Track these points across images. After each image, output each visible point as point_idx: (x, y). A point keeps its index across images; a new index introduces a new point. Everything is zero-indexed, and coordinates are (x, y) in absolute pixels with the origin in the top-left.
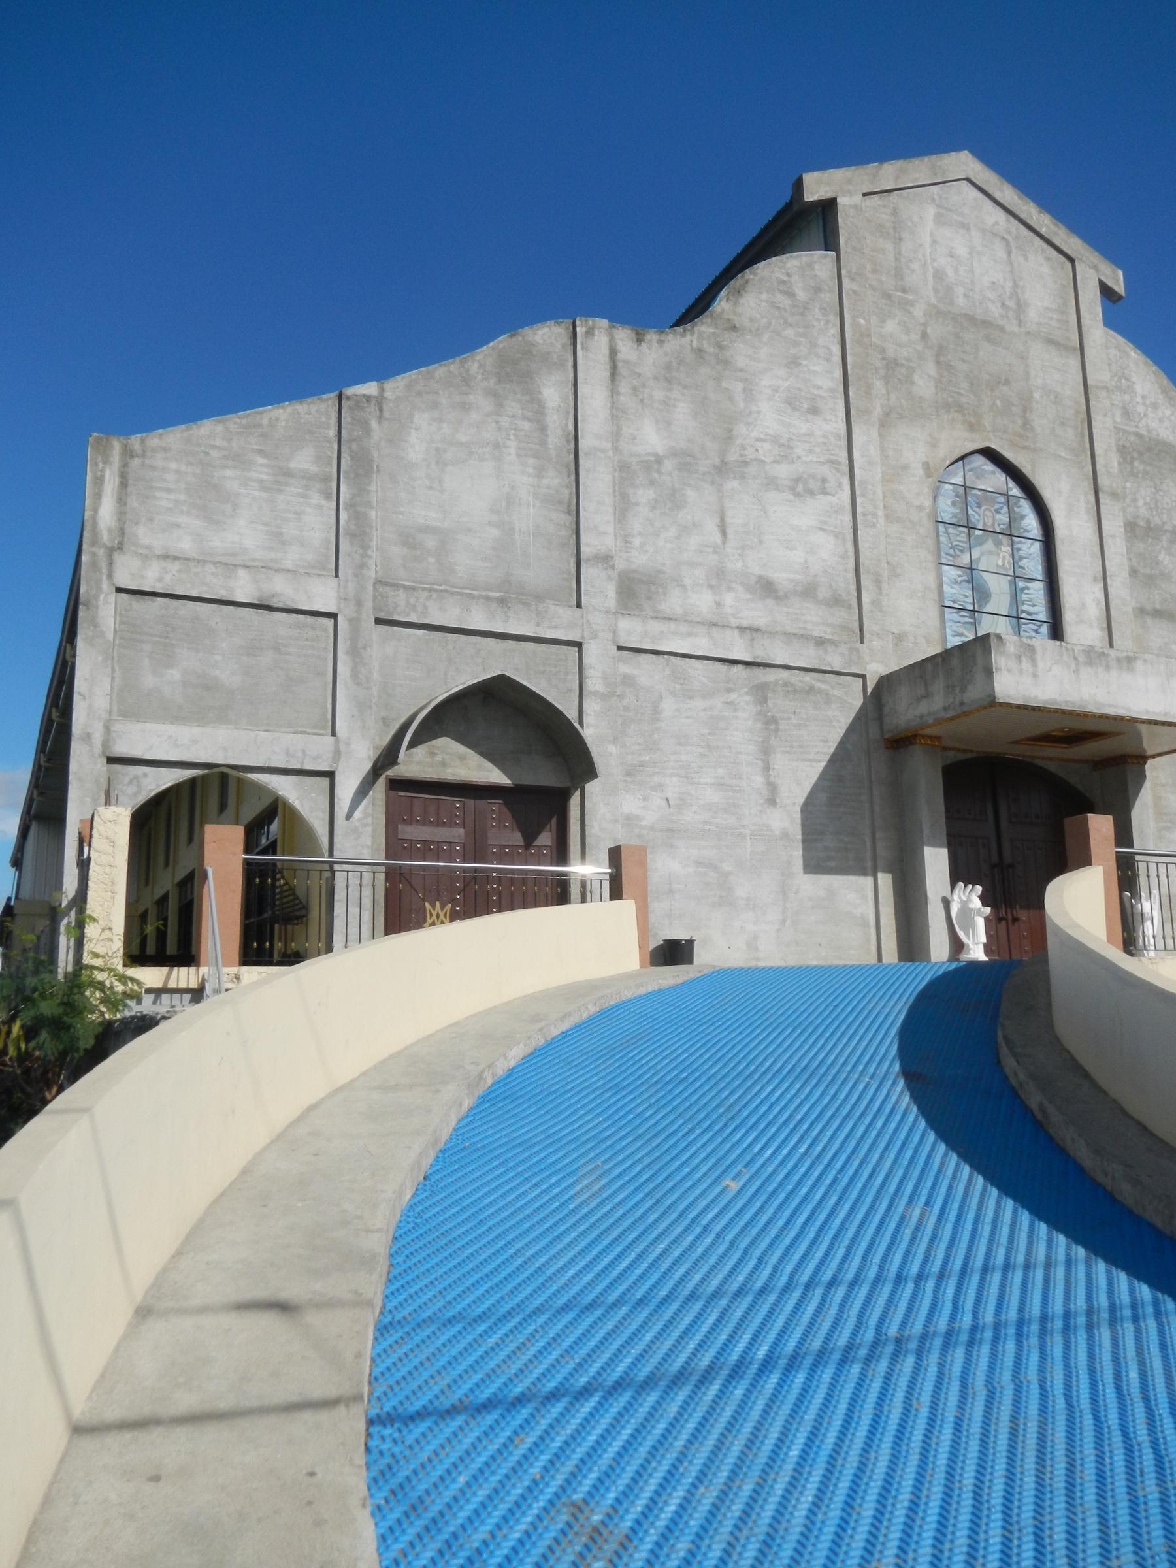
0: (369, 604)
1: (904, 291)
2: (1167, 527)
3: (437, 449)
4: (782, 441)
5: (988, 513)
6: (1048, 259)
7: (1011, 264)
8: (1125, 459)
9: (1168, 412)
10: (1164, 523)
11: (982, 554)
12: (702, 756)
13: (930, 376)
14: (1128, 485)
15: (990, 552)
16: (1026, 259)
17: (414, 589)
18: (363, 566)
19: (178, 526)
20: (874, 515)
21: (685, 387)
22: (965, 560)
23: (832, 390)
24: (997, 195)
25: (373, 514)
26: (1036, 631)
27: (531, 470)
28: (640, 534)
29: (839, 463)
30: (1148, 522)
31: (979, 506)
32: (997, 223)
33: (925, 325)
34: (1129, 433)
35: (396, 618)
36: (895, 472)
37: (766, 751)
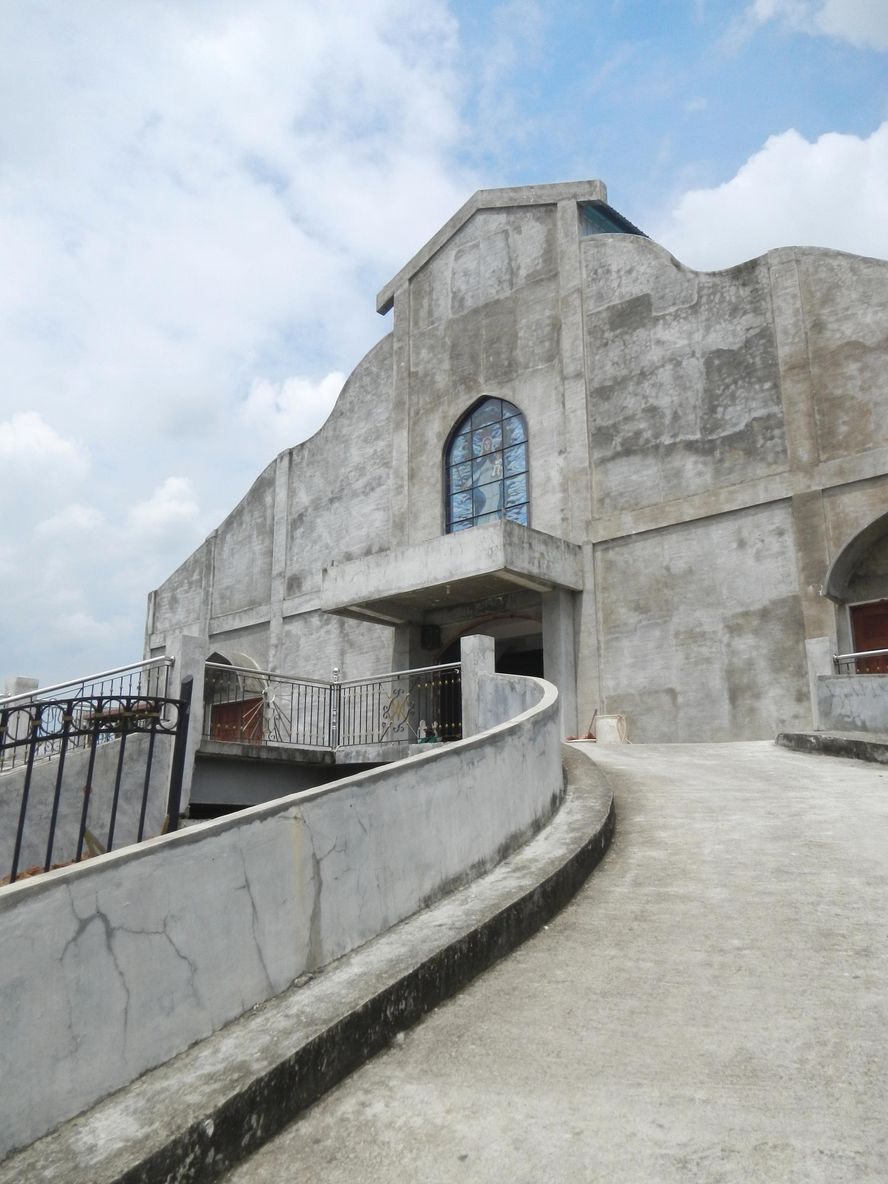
0: (207, 630)
1: (433, 323)
2: (633, 374)
3: (232, 549)
4: (361, 466)
5: (487, 442)
6: (538, 219)
7: (508, 246)
8: (596, 338)
9: (642, 269)
10: (631, 372)
11: (481, 474)
12: (315, 664)
13: (445, 371)
14: (597, 357)
15: (487, 470)
16: (520, 232)
17: (219, 617)
18: (207, 614)
19: (165, 618)
20: (402, 486)
21: (319, 462)
22: (469, 483)
23: (388, 419)
24: (498, 205)
25: (211, 589)
26: (518, 513)
27: (260, 542)
28: (297, 554)
29: (388, 462)
30: (615, 379)
31: (481, 440)
32: (500, 224)
33: (444, 338)
34: (599, 313)
35: (214, 633)
36: (416, 450)
37: (342, 653)
